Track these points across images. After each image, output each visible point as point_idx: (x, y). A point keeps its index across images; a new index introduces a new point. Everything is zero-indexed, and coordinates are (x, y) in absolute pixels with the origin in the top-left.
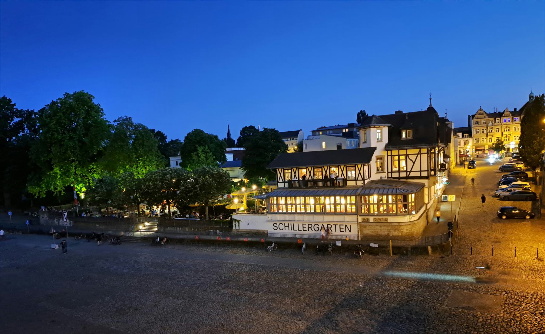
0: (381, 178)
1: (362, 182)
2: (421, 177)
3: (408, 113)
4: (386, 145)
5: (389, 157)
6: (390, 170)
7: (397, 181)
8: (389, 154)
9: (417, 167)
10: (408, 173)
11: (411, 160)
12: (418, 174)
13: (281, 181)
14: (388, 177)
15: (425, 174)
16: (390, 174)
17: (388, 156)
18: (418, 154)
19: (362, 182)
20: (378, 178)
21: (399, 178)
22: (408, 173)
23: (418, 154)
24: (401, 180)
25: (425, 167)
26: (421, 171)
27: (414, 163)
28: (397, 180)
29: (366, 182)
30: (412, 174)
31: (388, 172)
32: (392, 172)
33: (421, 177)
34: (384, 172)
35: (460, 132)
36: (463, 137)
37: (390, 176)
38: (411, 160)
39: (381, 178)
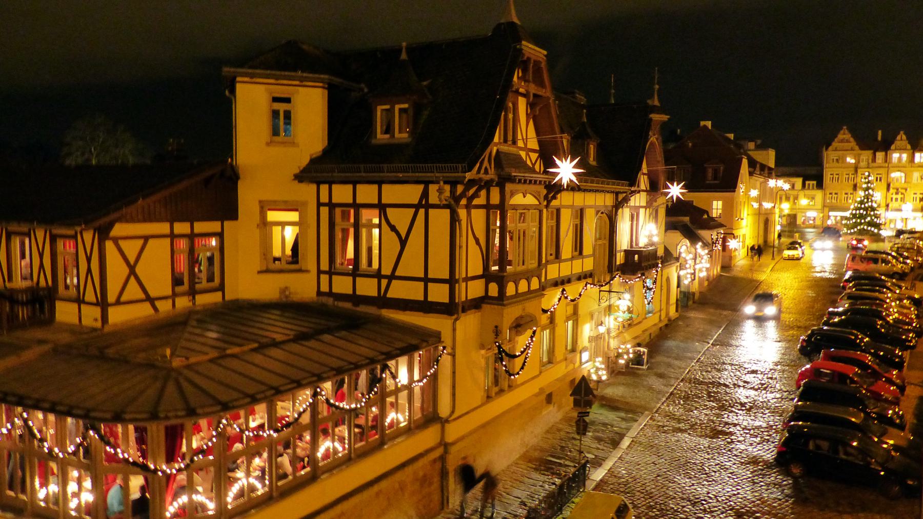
5: (325, 211)
6: (325, 266)
9: (412, 265)
10: (384, 282)
12: (414, 292)
14: (319, 293)
15: (439, 294)
16: (324, 278)
17: (319, 204)
21: (355, 299)
22: (384, 282)
23: (417, 207)
25: (440, 269)
27: (403, 243)
30: (398, 291)
31: (319, 272)
37: (325, 288)
39: (283, 291)
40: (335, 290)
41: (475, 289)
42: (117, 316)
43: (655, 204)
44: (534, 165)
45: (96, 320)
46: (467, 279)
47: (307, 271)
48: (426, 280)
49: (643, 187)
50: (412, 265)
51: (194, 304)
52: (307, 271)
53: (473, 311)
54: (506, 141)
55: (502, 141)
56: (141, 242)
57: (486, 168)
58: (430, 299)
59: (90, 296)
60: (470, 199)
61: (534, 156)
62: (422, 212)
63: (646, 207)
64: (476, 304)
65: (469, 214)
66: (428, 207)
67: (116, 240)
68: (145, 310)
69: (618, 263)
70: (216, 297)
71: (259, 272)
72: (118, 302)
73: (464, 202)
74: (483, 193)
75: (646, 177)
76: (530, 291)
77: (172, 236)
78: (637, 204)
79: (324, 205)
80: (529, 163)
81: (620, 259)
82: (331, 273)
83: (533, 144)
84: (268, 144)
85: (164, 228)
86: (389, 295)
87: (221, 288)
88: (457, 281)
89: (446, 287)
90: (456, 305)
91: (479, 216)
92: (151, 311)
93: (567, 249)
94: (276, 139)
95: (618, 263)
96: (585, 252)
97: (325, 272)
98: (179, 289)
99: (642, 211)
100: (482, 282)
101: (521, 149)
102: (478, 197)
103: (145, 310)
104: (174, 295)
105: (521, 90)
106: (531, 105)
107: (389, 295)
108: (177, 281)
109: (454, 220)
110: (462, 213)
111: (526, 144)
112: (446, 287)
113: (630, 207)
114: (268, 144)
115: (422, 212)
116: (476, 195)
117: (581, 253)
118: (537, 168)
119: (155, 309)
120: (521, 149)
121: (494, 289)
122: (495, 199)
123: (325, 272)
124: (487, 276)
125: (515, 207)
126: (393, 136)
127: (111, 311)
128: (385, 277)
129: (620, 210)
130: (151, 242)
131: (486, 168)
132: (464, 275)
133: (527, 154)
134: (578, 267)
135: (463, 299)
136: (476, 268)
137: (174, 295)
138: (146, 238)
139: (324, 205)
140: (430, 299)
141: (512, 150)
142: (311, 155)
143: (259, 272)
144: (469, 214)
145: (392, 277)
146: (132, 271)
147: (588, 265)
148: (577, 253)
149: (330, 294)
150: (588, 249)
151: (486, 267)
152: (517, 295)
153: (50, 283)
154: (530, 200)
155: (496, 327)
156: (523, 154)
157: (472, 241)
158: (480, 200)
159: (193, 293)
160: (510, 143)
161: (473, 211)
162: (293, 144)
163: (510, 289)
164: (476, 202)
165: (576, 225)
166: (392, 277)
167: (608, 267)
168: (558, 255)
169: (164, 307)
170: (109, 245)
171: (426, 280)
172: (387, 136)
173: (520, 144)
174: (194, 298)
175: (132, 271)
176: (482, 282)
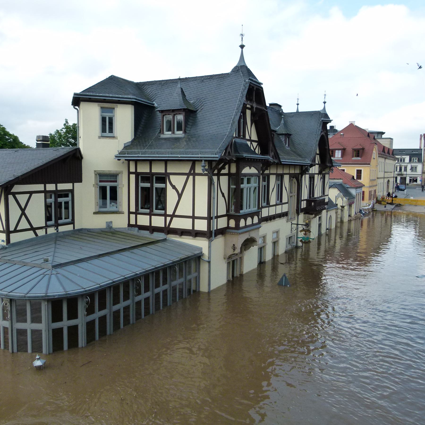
0: (109, 224)
2: (196, 234)
4: (126, 147)
5: (133, 177)
6: (133, 209)
8: (132, 169)
9: (185, 208)
10: (168, 219)
11: (174, 187)
12: (186, 224)
14: (129, 225)
15: (202, 226)
16: (133, 216)
17: (130, 173)
18: (188, 175)
20: (103, 226)
21: (153, 229)
22: (168, 219)
23: (188, 175)
25: (202, 210)
27: (180, 196)
28: (146, 233)
29: (15, 238)
30: (177, 224)
31: (130, 213)
33: (196, 234)
35: (407, 155)
36: (410, 160)
37: (133, 222)
38: (174, 187)
39: (109, 224)
40: (138, 223)
41: (222, 223)
42: (15, 238)
43: (324, 172)
44: (255, 149)
45: (3, 241)
46: (217, 217)
47: (122, 213)
48: (193, 217)
49: (317, 162)
50: (185, 208)
51: (57, 231)
52: (122, 213)
53: (220, 236)
54: (239, 135)
55: (237, 136)
56: (28, 195)
57: (229, 152)
58: (196, 229)
60: (219, 170)
61: (255, 144)
62: (191, 177)
63: (318, 174)
64: (222, 232)
65: (218, 179)
66: (195, 175)
67: (14, 194)
68: (30, 235)
69: (302, 207)
70: (70, 228)
71: (95, 213)
72: (16, 231)
73: (216, 172)
74: (227, 167)
75: (318, 156)
76: (253, 225)
77: (45, 192)
78: (313, 172)
79: (133, 173)
80: (252, 148)
81: (304, 205)
82: (136, 213)
83: (254, 137)
84: (99, 137)
85: (40, 187)
86: (171, 226)
87: (73, 222)
88: (212, 218)
89: (206, 221)
90: (211, 232)
91: (224, 180)
92: (34, 236)
93: (273, 200)
94: (105, 134)
95: (302, 207)
96: (284, 201)
97: (133, 213)
98: (49, 223)
99: (316, 176)
100: (226, 218)
101: (248, 140)
102: (224, 169)
103: (30, 235)
104: (46, 227)
105: (248, 106)
106: (252, 115)
107: (171, 226)
108: (48, 218)
109: (211, 183)
110: (215, 178)
111: (250, 138)
112: (206, 221)
113: (309, 174)
114: (99, 137)
115: (191, 177)
116: (223, 168)
117: (281, 201)
118: (257, 151)
119: (36, 234)
120: (248, 140)
121: (232, 223)
122: (233, 170)
123: (133, 213)
124: (229, 216)
125: (245, 175)
126: (173, 133)
127: (12, 235)
128: (169, 216)
129: (304, 176)
130: (33, 195)
131: (229, 152)
132: (216, 215)
133: (251, 143)
134: (279, 210)
135: (215, 229)
136: (222, 210)
137: (47, 226)
138: (31, 193)
139: (133, 173)
140: (196, 229)
141: (243, 141)
142: (125, 144)
143: (95, 213)
144: (218, 179)
145: (173, 216)
146: (23, 213)
147: (285, 208)
148: (279, 202)
149: (136, 225)
150: (285, 200)
151: (228, 211)
152: (246, 226)
154: (253, 171)
155: (234, 245)
156: (249, 143)
157: (220, 194)
158: (225, 171)
159: (57, 225)
160: (242, 137)
161: (221, 177)
162: (114, 137)
163: (242, 223)
164: (223, 172)
165: (279, 185)
166: (173, 216)
167: (297, 210)
168: (268, 203)
169: (41, 233)
170: (11, 197)
171: (193, 217)
172: (170, 133)
173: (247, 137)
174: (57, 228)
175: (23, 213)
176: (226, 218)
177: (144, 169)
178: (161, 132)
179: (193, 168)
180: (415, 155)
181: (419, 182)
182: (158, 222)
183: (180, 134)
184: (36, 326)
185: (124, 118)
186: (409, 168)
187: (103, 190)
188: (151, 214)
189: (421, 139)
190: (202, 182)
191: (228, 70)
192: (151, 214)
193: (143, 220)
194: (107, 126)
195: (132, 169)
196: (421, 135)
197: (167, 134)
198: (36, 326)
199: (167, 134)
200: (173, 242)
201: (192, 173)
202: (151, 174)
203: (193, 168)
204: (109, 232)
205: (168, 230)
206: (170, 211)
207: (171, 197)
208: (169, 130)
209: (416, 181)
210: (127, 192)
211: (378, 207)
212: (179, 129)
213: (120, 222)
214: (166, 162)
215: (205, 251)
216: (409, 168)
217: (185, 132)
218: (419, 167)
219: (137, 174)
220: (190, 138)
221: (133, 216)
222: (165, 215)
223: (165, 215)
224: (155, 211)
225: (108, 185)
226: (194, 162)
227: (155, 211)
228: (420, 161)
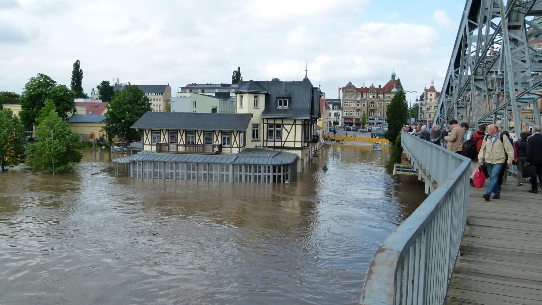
0: (256, 146)
1: (238, 149)
3: (286, 83)
4: (263, 113)
5: (265, 126)
6: (265, 139)
7: (271, 151)
8: (265, 122)
9: (291, 138)
10: (283, 143)
11: (286, 130)
12: (292, 145)
13: (147, 143)
14: (263, 146)
15: (299, 145)
16: (265, 143)
17: (264, 124)
18: (293, 125)
19: (238, 149)
20: (254, 147)
22: (283, 143)
24: (276, 150)
25: (299, 138)
26: (295, 142)
27: (289, 133)
28: (272, 149)
30: (287, 145)
31: (263, 141)
32: (267, 141)
34: (259, 141)
35: (331, 103)
36: (333, 108)
37: (265, 145)
38: (286, 130)
39: (256, 146)
50: (291, 138)
59: (235, 145)
66: (296, 124)
82: (267, 141)
145: (285, 141)
149: (267, 146)
153: (220, 143)
166: (285, 141)
171: (295, 142)
177: (270, 122)
178: (277, 106)
179: (295, 122)
180: (336, 103)
181: (340, 124)
182: (278, 144)
183: (286, 107)
184: (279, 174)
185: (262, 99)
186: (333, 114)
187: (254, 131)
188: (274, 141)
189: (339, 91)
190: (299, 129)
191: (302, 80)
192: (274, 141)
193: (271, 144)
194: (256, 104)
195: (265, 122)
196: (340, 89)
197: (280, 107)
198: (279, 174)
199: (280, 107)
200: (285, 153)
201: (295, 124)
202: (275, 124)
203: (295, 122)
204: (256, 150)
205: (283, 148)
206: (284, 140)
207: (285, 134)
208: (280, 105)
209: (338, 124)
210: (263, 132)
211: (329, 143)
212: (286, 105)
213: (259, 144)
214: (282, 119)
215: (300, 155)
216: (333, 114)
217: (289, 106)
218: (340, 113)
219: (267, 124)
220: (291, 109)
221: (265, 143)
222: (282, 141)
223: (282, 141)
224: (276, 140)
225: (255, 129)
226: (295, 120)
227: (276, 140)
228: (340, 108)
